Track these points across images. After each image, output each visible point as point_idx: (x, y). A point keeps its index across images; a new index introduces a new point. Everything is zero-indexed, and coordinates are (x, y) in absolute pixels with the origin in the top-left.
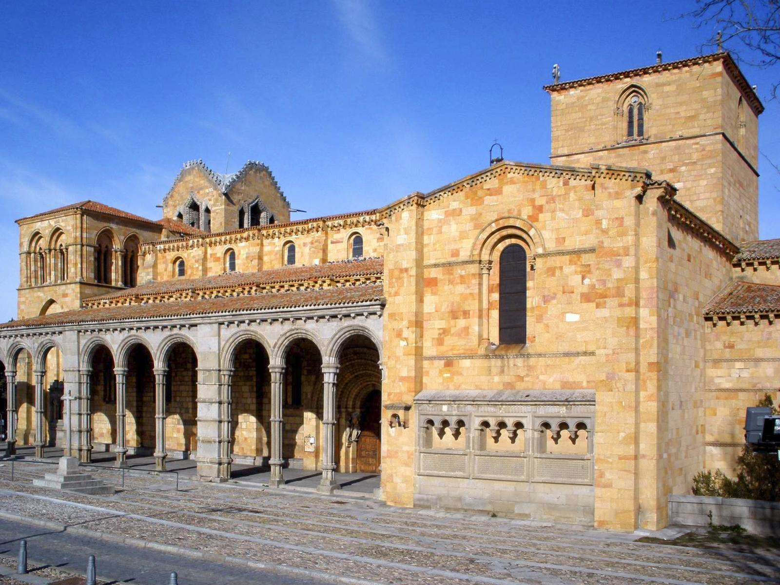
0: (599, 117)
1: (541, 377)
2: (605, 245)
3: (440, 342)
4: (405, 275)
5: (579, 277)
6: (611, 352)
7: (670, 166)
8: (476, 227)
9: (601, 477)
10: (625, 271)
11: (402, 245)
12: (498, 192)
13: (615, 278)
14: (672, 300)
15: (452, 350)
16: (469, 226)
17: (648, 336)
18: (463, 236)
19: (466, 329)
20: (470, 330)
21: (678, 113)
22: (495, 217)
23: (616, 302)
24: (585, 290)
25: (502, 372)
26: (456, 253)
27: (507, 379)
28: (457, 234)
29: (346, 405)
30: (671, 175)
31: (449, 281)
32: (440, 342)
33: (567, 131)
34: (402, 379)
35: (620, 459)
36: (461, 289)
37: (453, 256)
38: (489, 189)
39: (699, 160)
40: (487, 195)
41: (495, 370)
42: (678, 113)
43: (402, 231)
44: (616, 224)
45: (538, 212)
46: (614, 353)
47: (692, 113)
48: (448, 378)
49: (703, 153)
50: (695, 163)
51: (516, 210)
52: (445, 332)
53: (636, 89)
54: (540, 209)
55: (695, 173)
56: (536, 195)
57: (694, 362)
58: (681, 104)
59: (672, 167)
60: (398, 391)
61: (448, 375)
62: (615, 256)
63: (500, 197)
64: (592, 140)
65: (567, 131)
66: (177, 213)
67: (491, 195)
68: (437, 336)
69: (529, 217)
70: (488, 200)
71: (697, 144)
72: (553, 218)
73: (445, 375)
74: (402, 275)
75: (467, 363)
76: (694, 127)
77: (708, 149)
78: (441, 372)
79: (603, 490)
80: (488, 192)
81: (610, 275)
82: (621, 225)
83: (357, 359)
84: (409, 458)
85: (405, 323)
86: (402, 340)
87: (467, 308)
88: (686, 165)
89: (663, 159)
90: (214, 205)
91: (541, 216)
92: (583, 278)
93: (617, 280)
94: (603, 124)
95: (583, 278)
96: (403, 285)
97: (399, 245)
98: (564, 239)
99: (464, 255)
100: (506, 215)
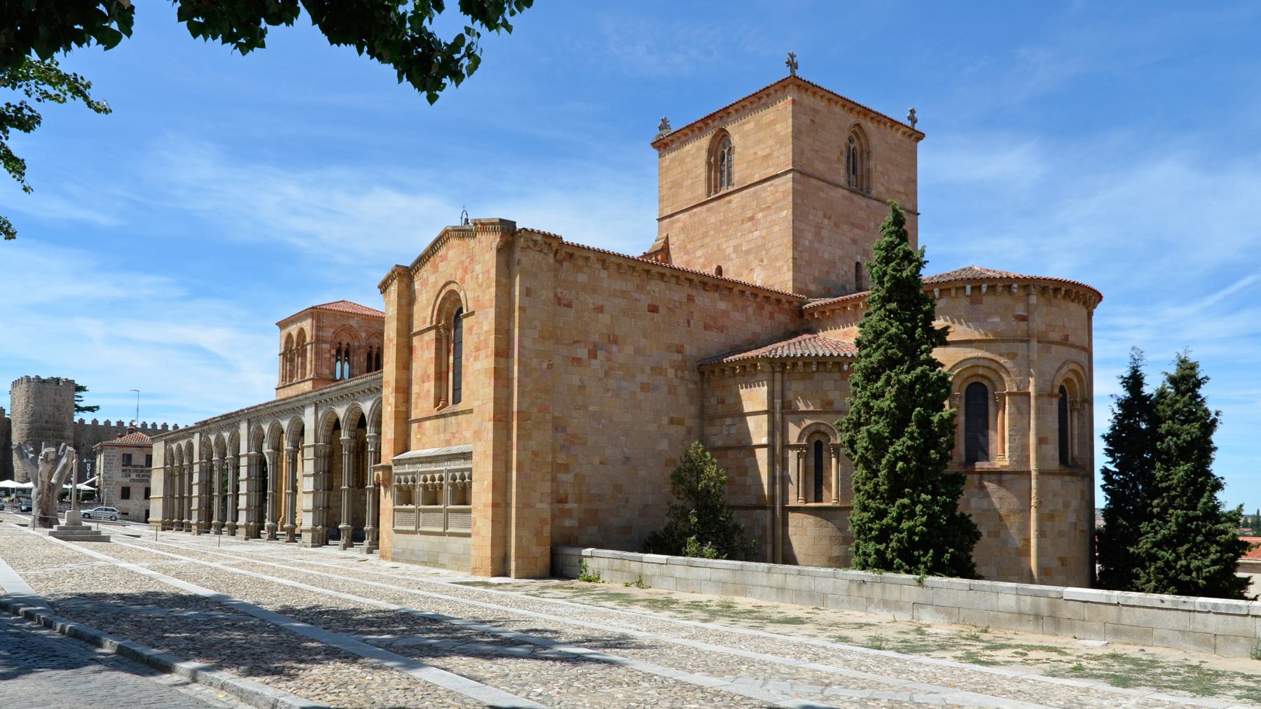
7: (749, 214)
27: (448, 436)
28: (425, 302)
30: (750, 224)
33: (670, 189)
39: (773, 204)
41: (442, 429)
47: (767, 151)
49: (777, 195)
55: (769, 219)
58: (759, 142)
59: (750, 215)
64: (689, 195)
71: (772, 185)
75: (428, 423)
76: (769, 167)
77: (781, 189)
87: (429, 372)
88: (762, 210)
89: (743, 207)
100: (449, 279)
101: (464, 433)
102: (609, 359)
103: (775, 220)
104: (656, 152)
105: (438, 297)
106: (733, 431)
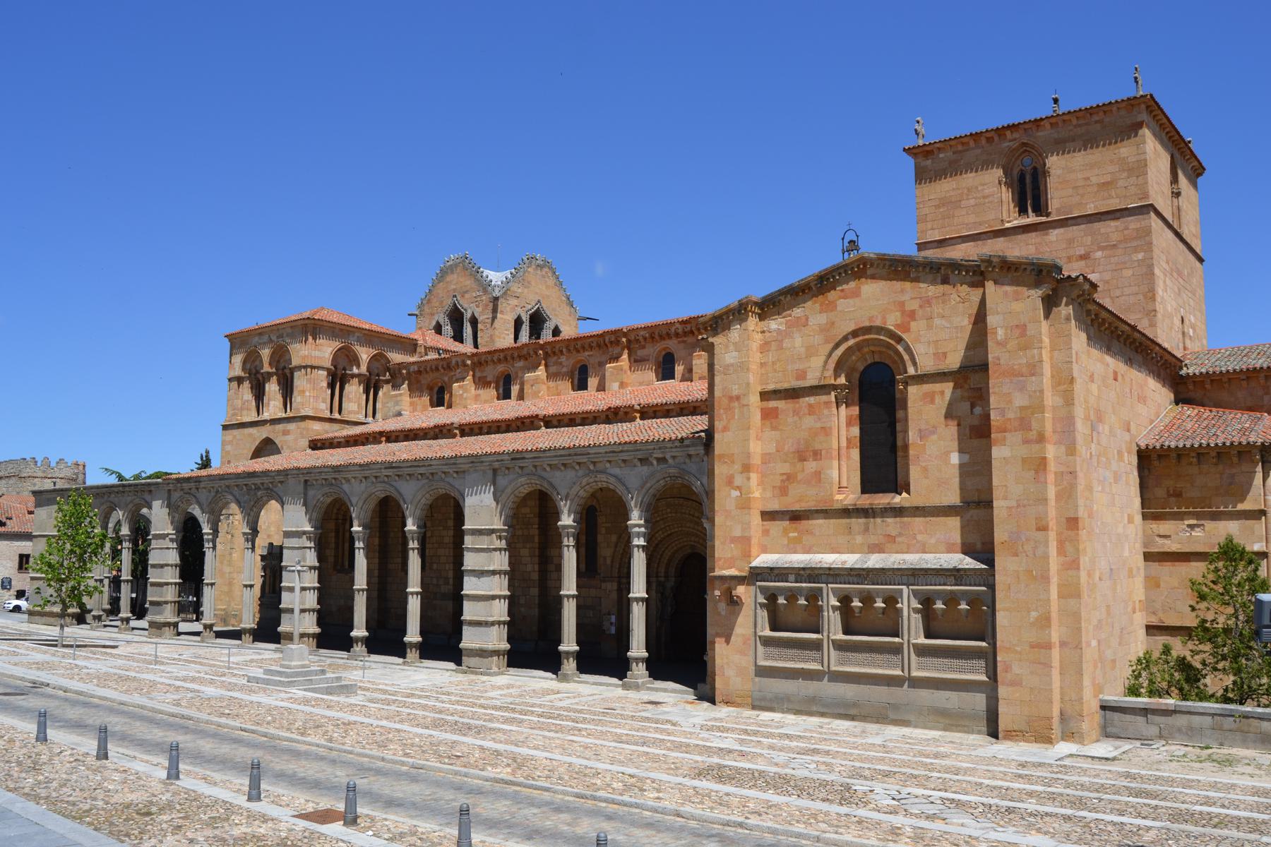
0: (979, 188)
1: (919, 537)
2: (1002, 362)
3: (783, 491)
4: (736, 404)
5: (967, 405)
6: (1014, 504)
8: (827, 342)
9: (1006, 672)
10: (1030, 396)
11: (732, 365)
12: (856, 294)
13: (1017, 405)
14: (1095, 434)
15: (800, 501)
16: (818, 339)
17: (1065, 482)
18: (810, 352)
19: (818, 475)
20: (822, 476)
21: (1087, 179)
22: (852, 327)
23: (1020, 436)
24: (976, 422)
25: (867, 529)
26: (802, 375)
27: (873, 539)
28: (803, 350)
29: (657, 573)
30: (1083, 263)
31: (794, 411)
32: (783, 491)
33: (937, 207)
34: (734, 540)
35: (1032, 647)
36: (809, 422)
37: (798, 379)
38: (842, 290)
39: (1120, 241)
40: (841, 298)
42: (1088, 178)
43: (732, 347)
44: (1017, 332)
45: (908, 319)
46: (1018, 506)
47: (1108, 178)
48: (795, 537)
49: (1126, 232)
50: (1114, 245)
51: (880, 318)
52: (789, 478)
53: (1028, 149)
54: (912, 315)
55: (1113, 260)
56: (906, 297)
57: (1126, 515)
60: (729, 556)
61: (796, 534)
62: (1016, 376)
63: (857, 300)
65: (937, 207)
66: (434, 323)
67: (845, 298)
68: (779, 484)
69: (897, 326)
70: (842, 304)
72: (930, 327)
73: (791, 535)
74: (732, 405)
76: (1111, 197)
77: (1132, 226)
78: (785, 531)
79: (1010, 689)
80: (842, 294)
81: (1010, 402)
82: (1023, 334)
83: (671, 513)
84: (744, 643)
85: (737, 467)
86: (733, 489)
87: (817, 446)
88: (1102, 249)
89: (1070, 242)
90: (482, 313)
91: (913, 325)
92: (973, 406)
93: (1022, 408)
94: (984, 197)
95: (973, 406)
96: (733, 417)
97: (728, 365)
98: (945, 354)
99: (811, 380)
101: (919, 537)
102: (1099, 444)
103: (1125, 263)
104: (910, 162)
105: (837, 346)
106: (1197, 533)
